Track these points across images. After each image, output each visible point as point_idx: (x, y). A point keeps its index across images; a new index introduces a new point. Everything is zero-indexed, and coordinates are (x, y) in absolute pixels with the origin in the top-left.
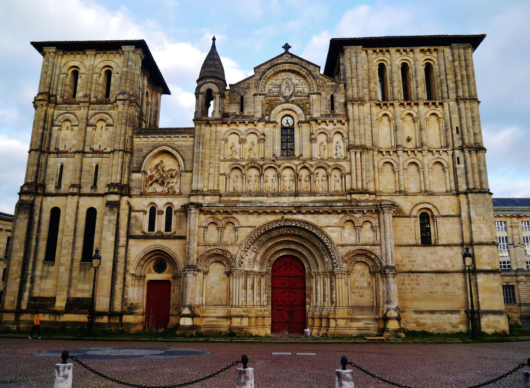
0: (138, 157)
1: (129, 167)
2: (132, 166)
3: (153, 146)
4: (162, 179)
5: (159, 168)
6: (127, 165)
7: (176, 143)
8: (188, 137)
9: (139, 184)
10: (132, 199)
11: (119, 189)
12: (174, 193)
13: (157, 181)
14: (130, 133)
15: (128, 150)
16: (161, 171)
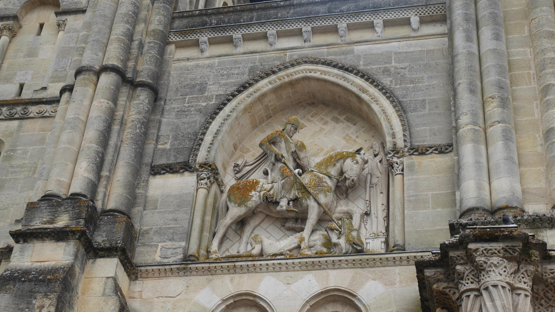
0: (182, 113)
1: (139, 154)
2: (150, 147)
3: (252, 70)
4: (295, 193)
5: (282, 149)
6: (128, 133)
7: (358, 48)
8: (415, 20)
9: (184, 216)
10: (138, 286)
11: (77, 217)
12: (357, 249)
13: (270, 202)
14: (157, 20)
15: (143, 78)
16: (291, 165)
